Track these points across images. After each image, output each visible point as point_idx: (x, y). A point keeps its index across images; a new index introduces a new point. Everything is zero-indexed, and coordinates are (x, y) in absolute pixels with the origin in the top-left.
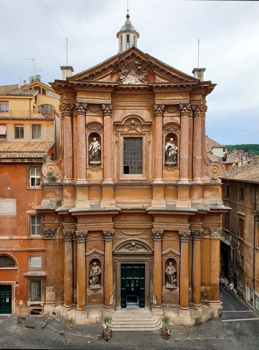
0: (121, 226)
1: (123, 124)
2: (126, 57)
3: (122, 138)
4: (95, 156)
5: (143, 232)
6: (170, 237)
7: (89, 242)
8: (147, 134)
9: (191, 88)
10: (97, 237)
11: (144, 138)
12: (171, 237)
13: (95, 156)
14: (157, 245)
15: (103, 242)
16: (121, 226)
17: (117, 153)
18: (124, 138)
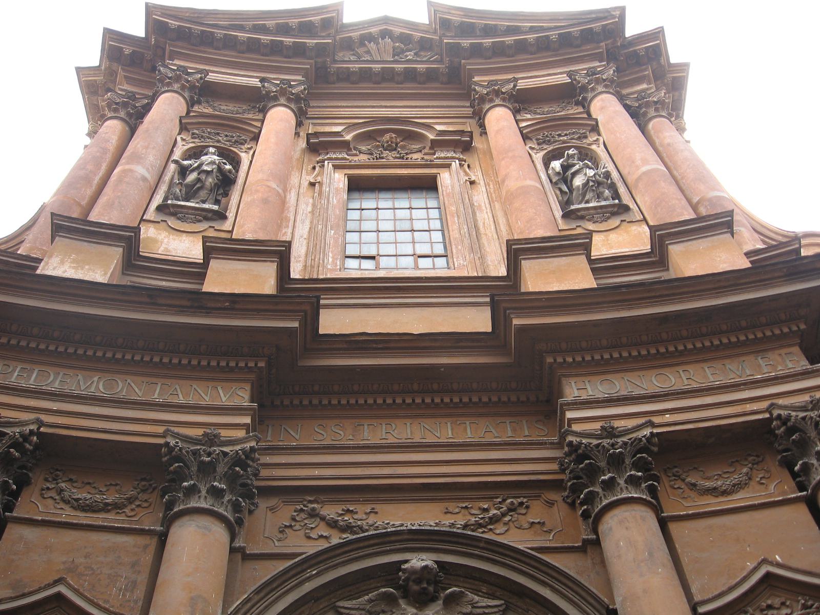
0: (316, 472)
1: (348, 137)
2: (362, 32)
3: (340, 180)
4: (198, 185)
5: (494, 512)
6: (714, 492)
7: (29, 533)
8: (455, 165)
9: (603, 44)
10: (106, 508)
11: (445, 179)
12: (725, 493)
13: (198, 185)
14: (629, 534)
15: (146, 547)
16: (316, 472)
17: (312, 212)
18: (357, 186)
